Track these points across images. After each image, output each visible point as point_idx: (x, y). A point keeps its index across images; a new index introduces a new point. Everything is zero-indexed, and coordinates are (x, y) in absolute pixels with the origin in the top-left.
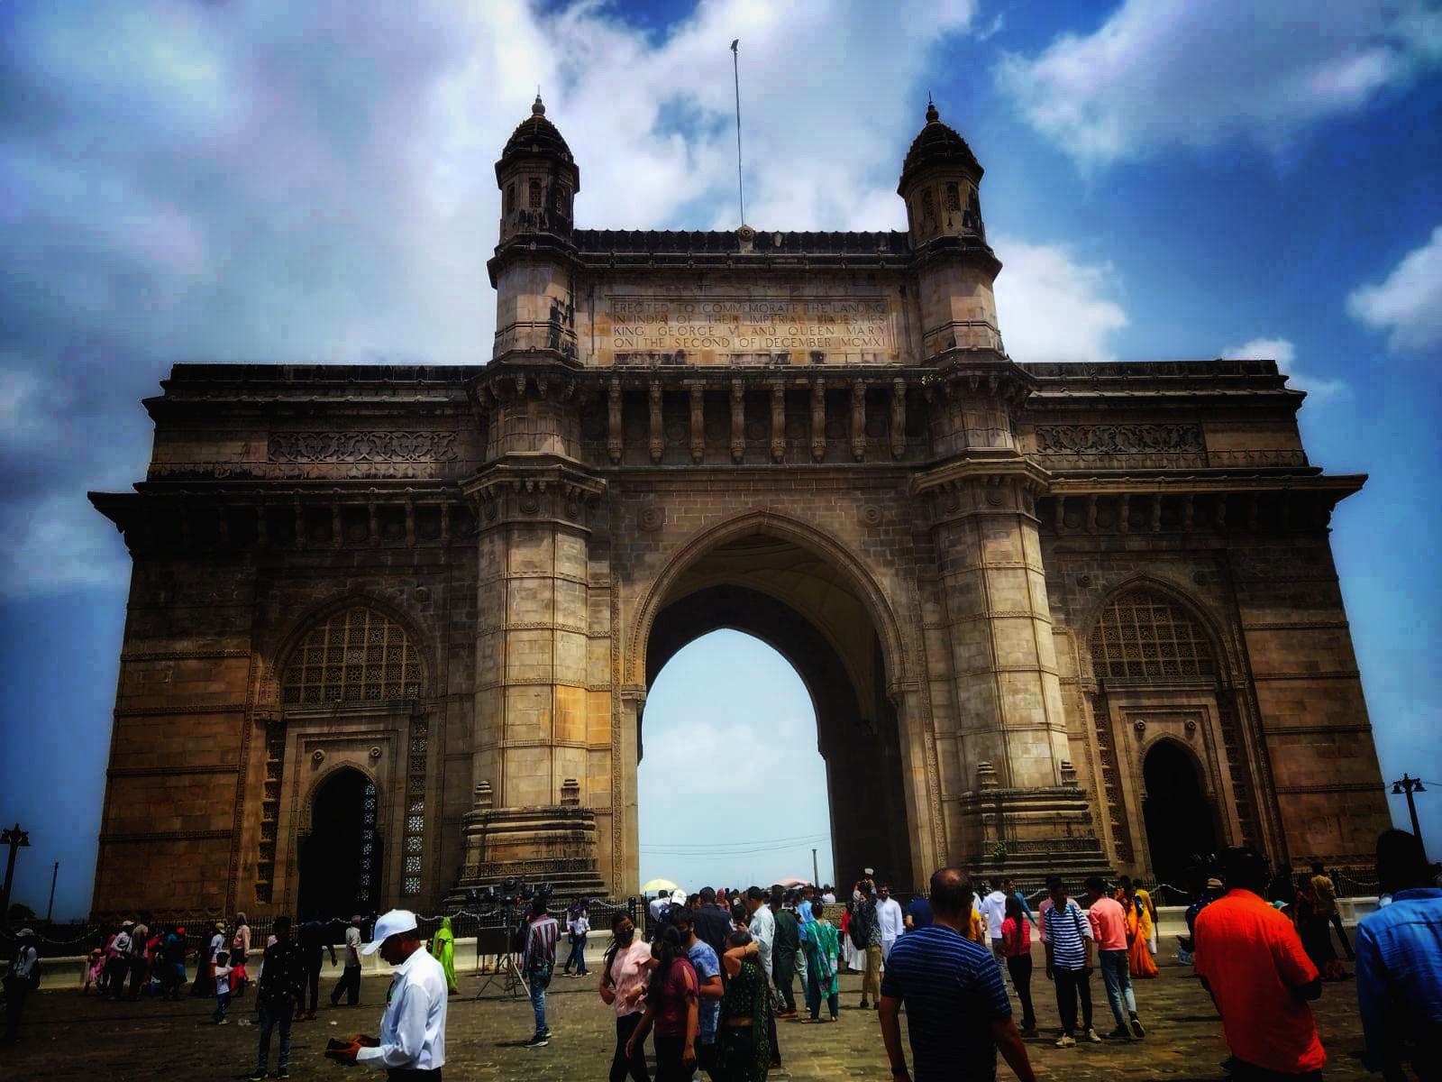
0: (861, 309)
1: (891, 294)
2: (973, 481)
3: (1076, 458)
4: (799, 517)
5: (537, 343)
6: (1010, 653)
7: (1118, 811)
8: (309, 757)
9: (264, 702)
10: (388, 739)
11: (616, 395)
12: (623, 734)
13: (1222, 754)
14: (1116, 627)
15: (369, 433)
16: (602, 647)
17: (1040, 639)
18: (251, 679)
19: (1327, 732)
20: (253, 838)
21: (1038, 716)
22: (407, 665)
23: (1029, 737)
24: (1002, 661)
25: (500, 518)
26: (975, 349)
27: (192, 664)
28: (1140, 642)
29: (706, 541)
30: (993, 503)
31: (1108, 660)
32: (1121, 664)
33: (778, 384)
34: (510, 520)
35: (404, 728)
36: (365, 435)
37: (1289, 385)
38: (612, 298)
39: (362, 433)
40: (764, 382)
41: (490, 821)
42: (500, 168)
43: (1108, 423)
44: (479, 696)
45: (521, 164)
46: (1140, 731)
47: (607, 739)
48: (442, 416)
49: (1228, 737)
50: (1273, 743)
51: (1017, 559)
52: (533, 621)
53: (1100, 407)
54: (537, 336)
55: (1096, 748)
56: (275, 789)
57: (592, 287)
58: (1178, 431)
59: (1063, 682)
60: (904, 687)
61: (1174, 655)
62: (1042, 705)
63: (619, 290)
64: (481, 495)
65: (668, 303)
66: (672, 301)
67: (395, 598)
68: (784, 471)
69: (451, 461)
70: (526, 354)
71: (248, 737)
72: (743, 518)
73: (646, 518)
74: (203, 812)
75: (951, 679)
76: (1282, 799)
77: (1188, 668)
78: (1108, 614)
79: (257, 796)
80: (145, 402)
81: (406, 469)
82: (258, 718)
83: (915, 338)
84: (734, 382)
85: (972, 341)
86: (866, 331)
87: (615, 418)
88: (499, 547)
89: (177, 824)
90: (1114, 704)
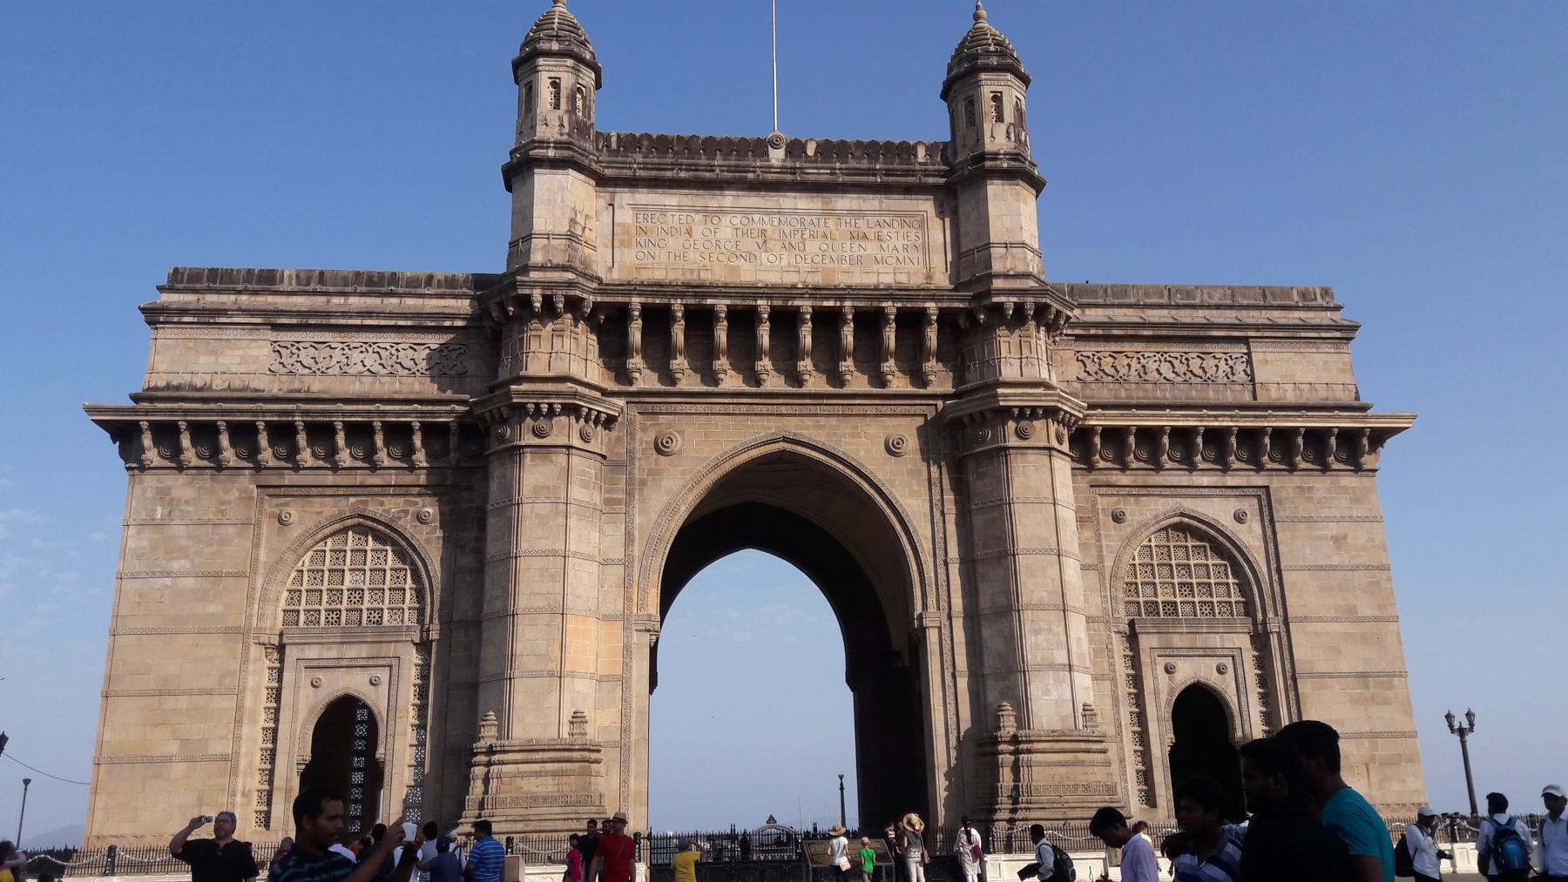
0: (896, 224)
2: (1006, 413)
3: (1117, 386)
4: (824, 444)
5: (553, 257)
6: (1033, 592)
7: (1145, 755)
9: (262, 625)
10: (390, 666)
11: (637, 313)
12: (634, 667)
14: (1152, 565)
15: (374, 343)
17: (1066, 578)
18: (250, 597)
19: (1364, 675)
20: (251, 763)
21: (1061, 658)
26: (1012, 273)
27: (189, 582)
28: (1176, 581)
29: (727, 467)
32: (1157, 602)
34: (523, 443)
36: (370, 346)
38: (635, 207)
39: (366, 343)
40: (790, 304)
41: (495, 753)
42: (517, 65)
43: (1152, 349)
44: (485, 625)
45: (541, 61)
46: (1169, 670)
47: (619, 671)
50: (1304, 687)
51: (1047, 493)
52: (544, 548)
53: (1146, 333)
54: (554, 248)
58: (1226, 360)
59: (1089, 620)
61: (1211, 595)
62: (1065, 646)
63: (644, 197)
64: (493, 417)
65: (693, 214)
67: (401, 518)
70: (543, 268)
71: (246, 661)
73: (664, 442)
74: (201, 736)
77: (1224, 610)
79: (254, 721)
80: (139, 308)
81: (413, 383)
82: (255, 641)
84: (759, 302)
85: (1009, 267)
86: (900, 247)
89: (173, 748)
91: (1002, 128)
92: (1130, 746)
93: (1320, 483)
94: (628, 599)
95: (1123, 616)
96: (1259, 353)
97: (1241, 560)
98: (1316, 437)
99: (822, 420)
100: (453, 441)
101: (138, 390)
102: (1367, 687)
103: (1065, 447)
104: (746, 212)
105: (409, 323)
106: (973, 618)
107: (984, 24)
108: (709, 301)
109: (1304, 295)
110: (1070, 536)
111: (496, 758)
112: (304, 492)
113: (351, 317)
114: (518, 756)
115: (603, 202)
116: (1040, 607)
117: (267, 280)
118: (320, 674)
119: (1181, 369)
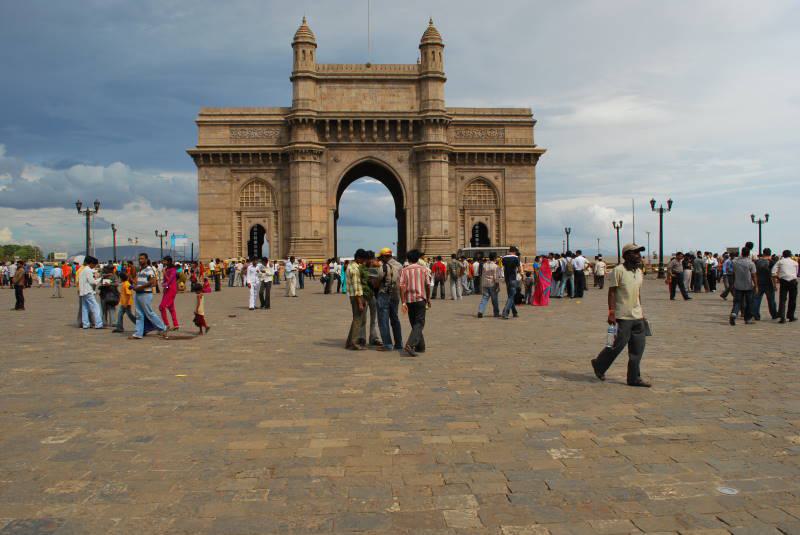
1: (413, 87)
2: (429, 151)
16: (324, 195)
21: (439, 217)
27: (216, 196)
42: (293, 45)
46: (473, 219)
47: (325, 219)
49: (498, 221)
50: (508, 224)
83: (419, 102)
89: (217, 237)
90: (466, 212)
96: (507, 130)
98: (518, 155)
104: (357, 88)
106: (419, 206)
107: (434, 26)
109: (524, 110)
110: (446, 185)
116: (435, 204)
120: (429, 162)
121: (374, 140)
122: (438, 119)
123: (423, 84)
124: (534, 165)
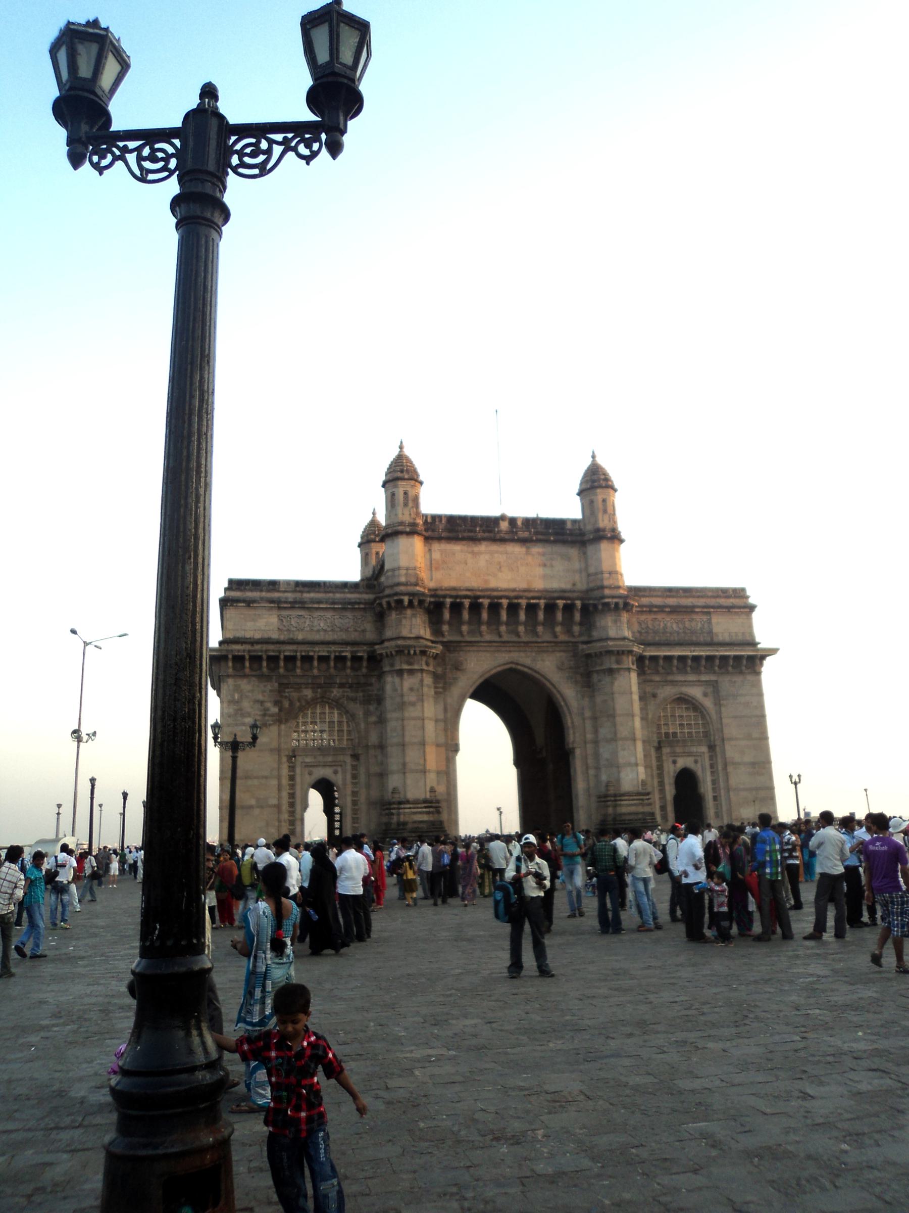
1: (573, 552)
2: (610, 653)
7: (663, 798)
8: (306, 773)
10: (341, 766)
13: (708, 773)
16: (441, 725)
19: (753, 764)
21: (633, 760)
22: (347, 730)
23: (629, 769)
24: (619, 736)
25: (397, 667)
28: (678, 723)
30: (618, 662)
31: (663, 731)
33: (523, 602)
35: (348, 760)
37: (751, 601)
40: (516, 601)
44: (389, 749)
46: (674, 762)
47: (444, 768)
48: (359, 608)
49: (712, 766)
50: (730, 769)
55: (655, 772)
56: (292, 786)
57: (431, 544)
59: (644, 742)
60: (575, 745)
64: (387, 656)
66: (469, 553)
68: (524, 642)
69: (364, 631)
72: (505, 664)
75: (596, 742)
76: (731, 793)
78: (665, 709)
83: (584, 575)
87: (447, 615)
88: (397, 680)
89: (253, 802)
91: (606, 518)
92: (656, 796)
93: (738, 679)
94: (446, 736)
95: (655, 738)
97: (705, 713)
98: (738, 658)
99: (529, 654)
100: (365, 664)
101: (221, 638)
102: (755, 768)
103: (635, 667)
105: (340, 606)
108: (481, 600)
109: (735, 590)
111: (402, 806)
112: (298, 687)
113: (314, 603)
114: (411, 806)
115: (427, 549)
117: (273, 585)
118: (311, 769)
119: (681, 626)
120: (611, 671)
121: (518, 634)
122: (621, 601)
123: (590, 549)
124: (758, 673)
